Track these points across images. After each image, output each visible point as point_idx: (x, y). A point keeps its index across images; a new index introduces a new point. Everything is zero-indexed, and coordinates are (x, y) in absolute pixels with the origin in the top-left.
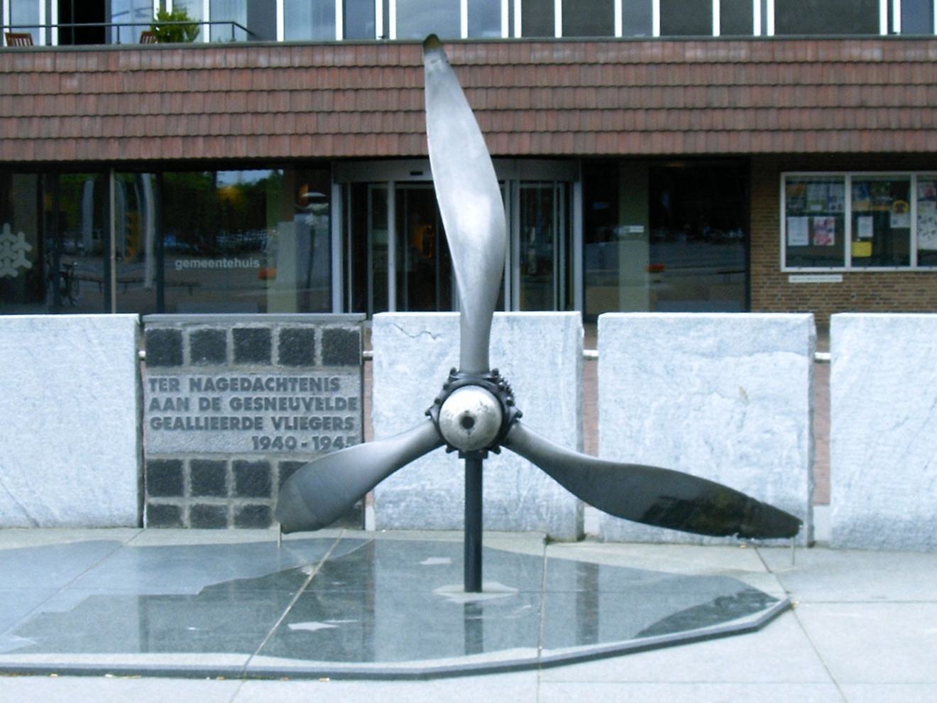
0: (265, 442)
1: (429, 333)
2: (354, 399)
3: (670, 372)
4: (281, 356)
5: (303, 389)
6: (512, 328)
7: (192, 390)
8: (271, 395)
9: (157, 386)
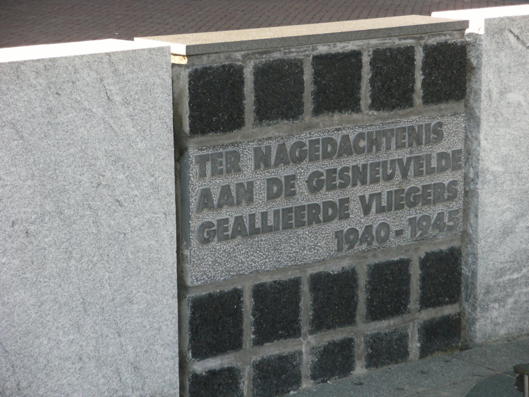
0: (352, 237)
2: (460, 151)
4: (374, 98)
5: (400, 146)
7: (257, 167)
8: (360, 161)
9: (209, 166)
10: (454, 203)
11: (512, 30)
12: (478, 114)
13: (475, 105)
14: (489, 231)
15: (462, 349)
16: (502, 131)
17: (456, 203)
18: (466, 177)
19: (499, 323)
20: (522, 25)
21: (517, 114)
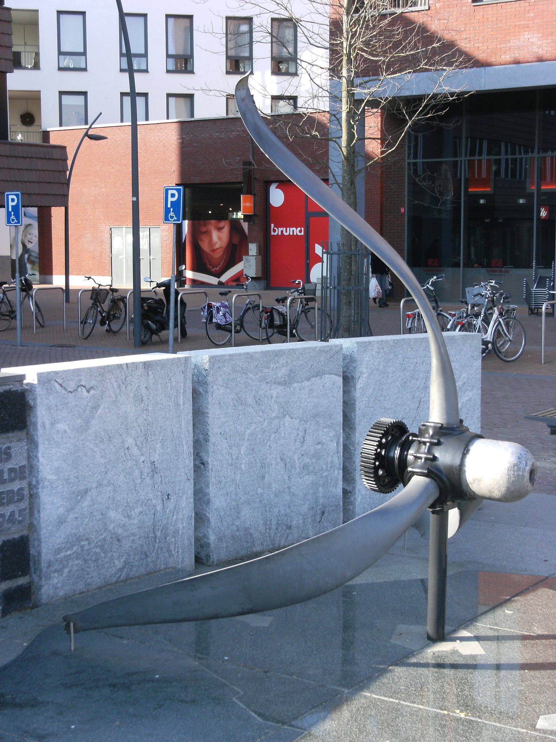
1: (85, 387)
2: (24, 466)
3: (258, 402)
6: (148, 375)
10: (22, 504)
11: (57, 380)
12: (36, 439)
13: (34, 433)
14: (48, 522)
15: (32, 608)
16: (54, 451)
17: (24, 503)
18: (30, 484)
19: (58, 588)
20: (64, 376)
21: (64, 438)
